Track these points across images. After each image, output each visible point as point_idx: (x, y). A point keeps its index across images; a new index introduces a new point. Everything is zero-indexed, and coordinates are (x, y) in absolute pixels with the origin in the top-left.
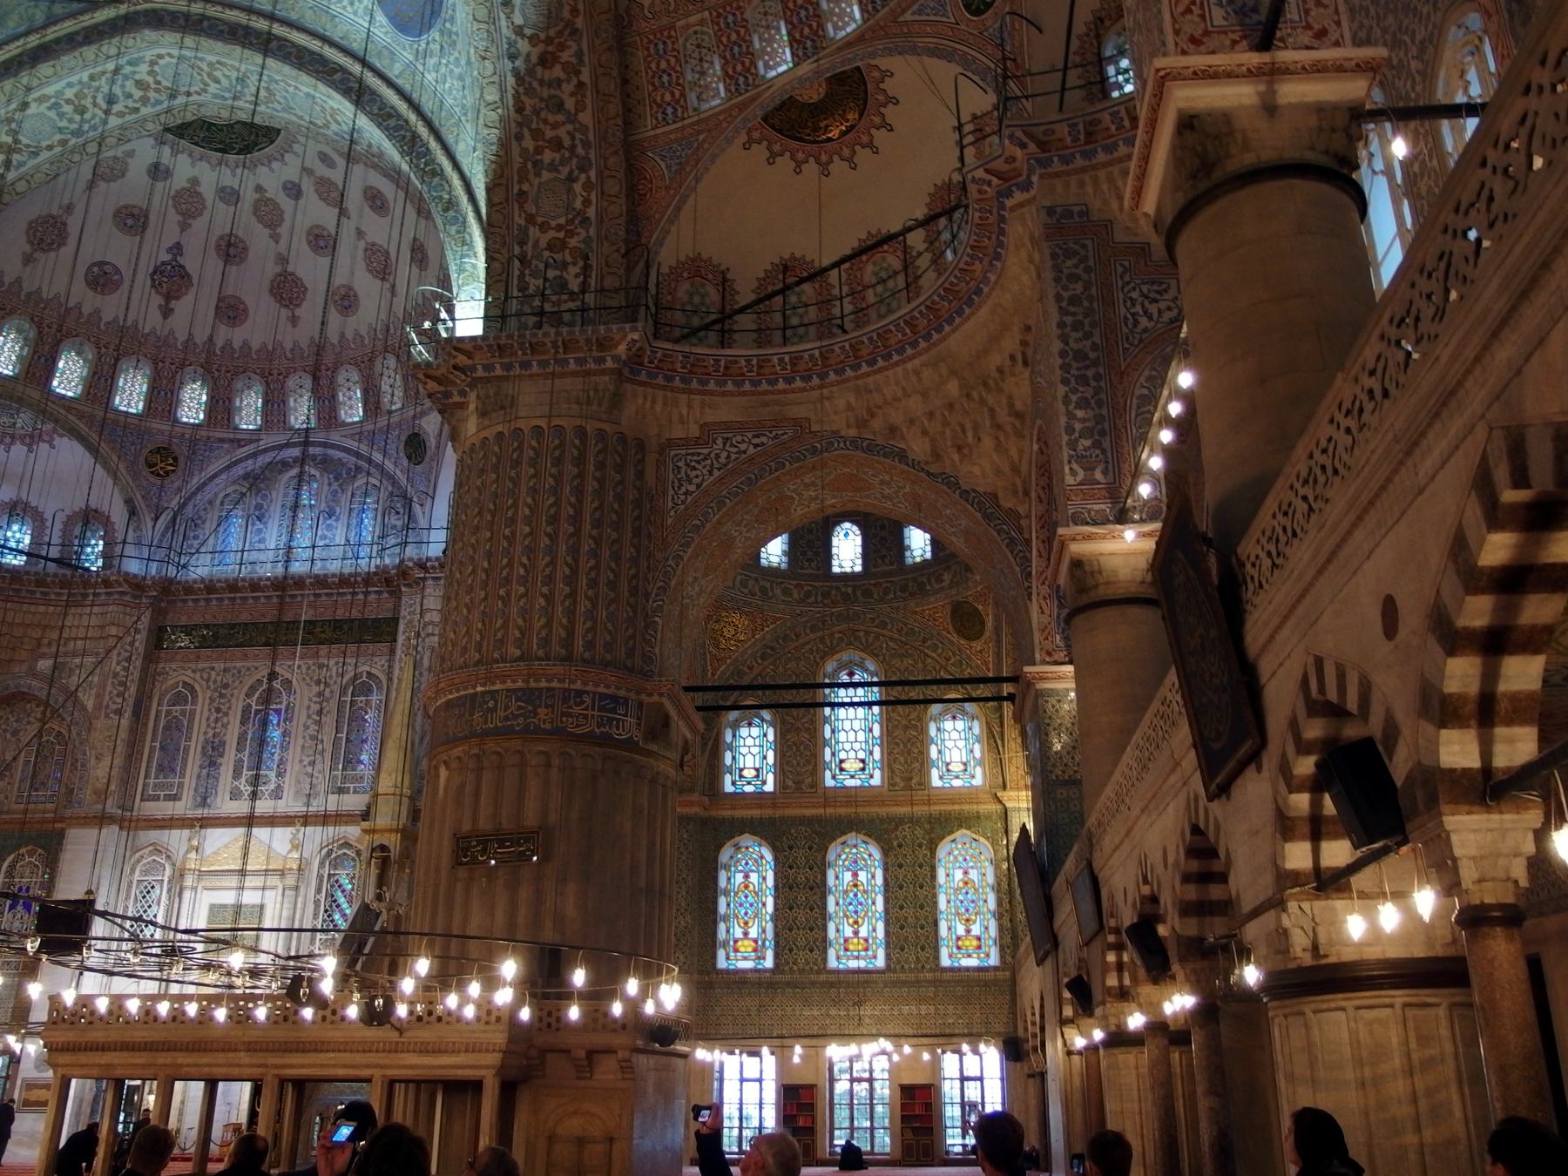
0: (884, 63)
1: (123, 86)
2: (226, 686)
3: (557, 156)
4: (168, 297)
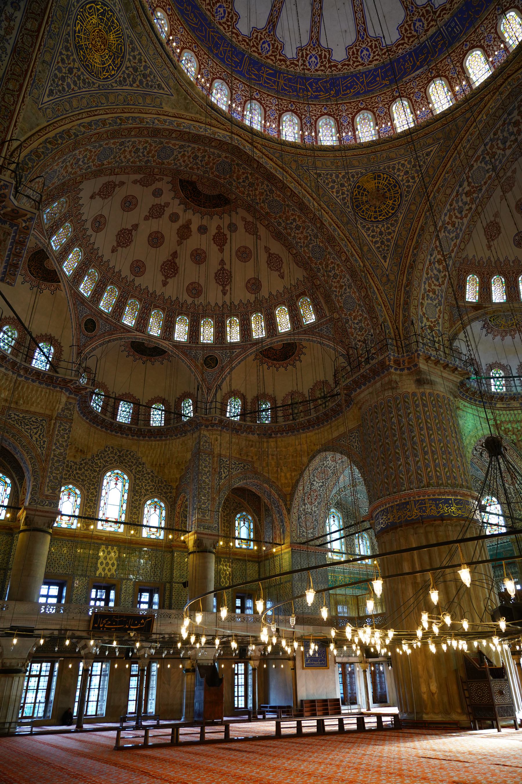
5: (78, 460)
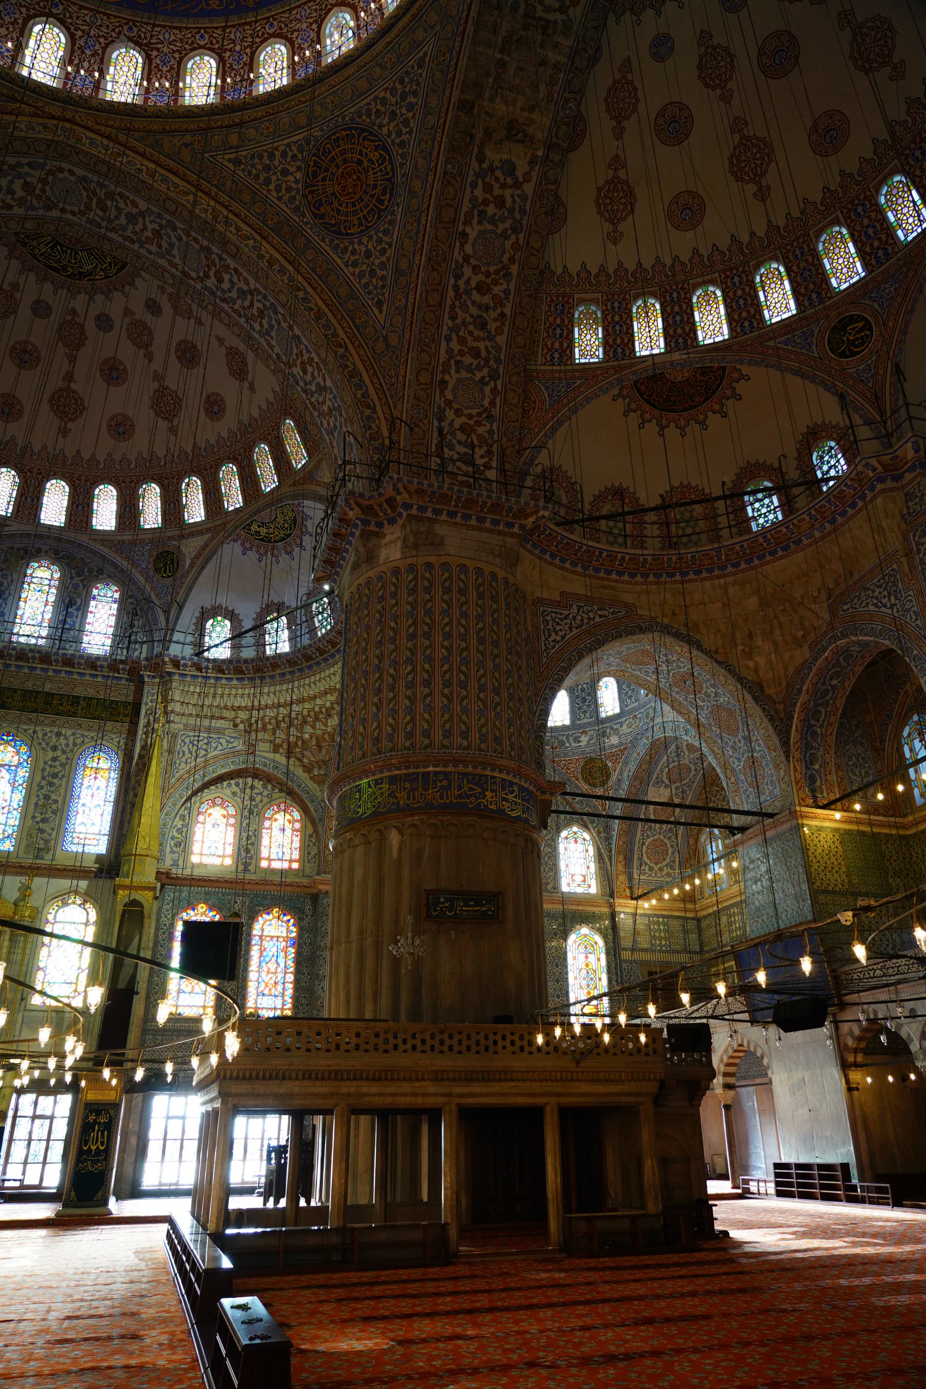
0: (745, 369)
1: (12, 182)
3: (475, 362)
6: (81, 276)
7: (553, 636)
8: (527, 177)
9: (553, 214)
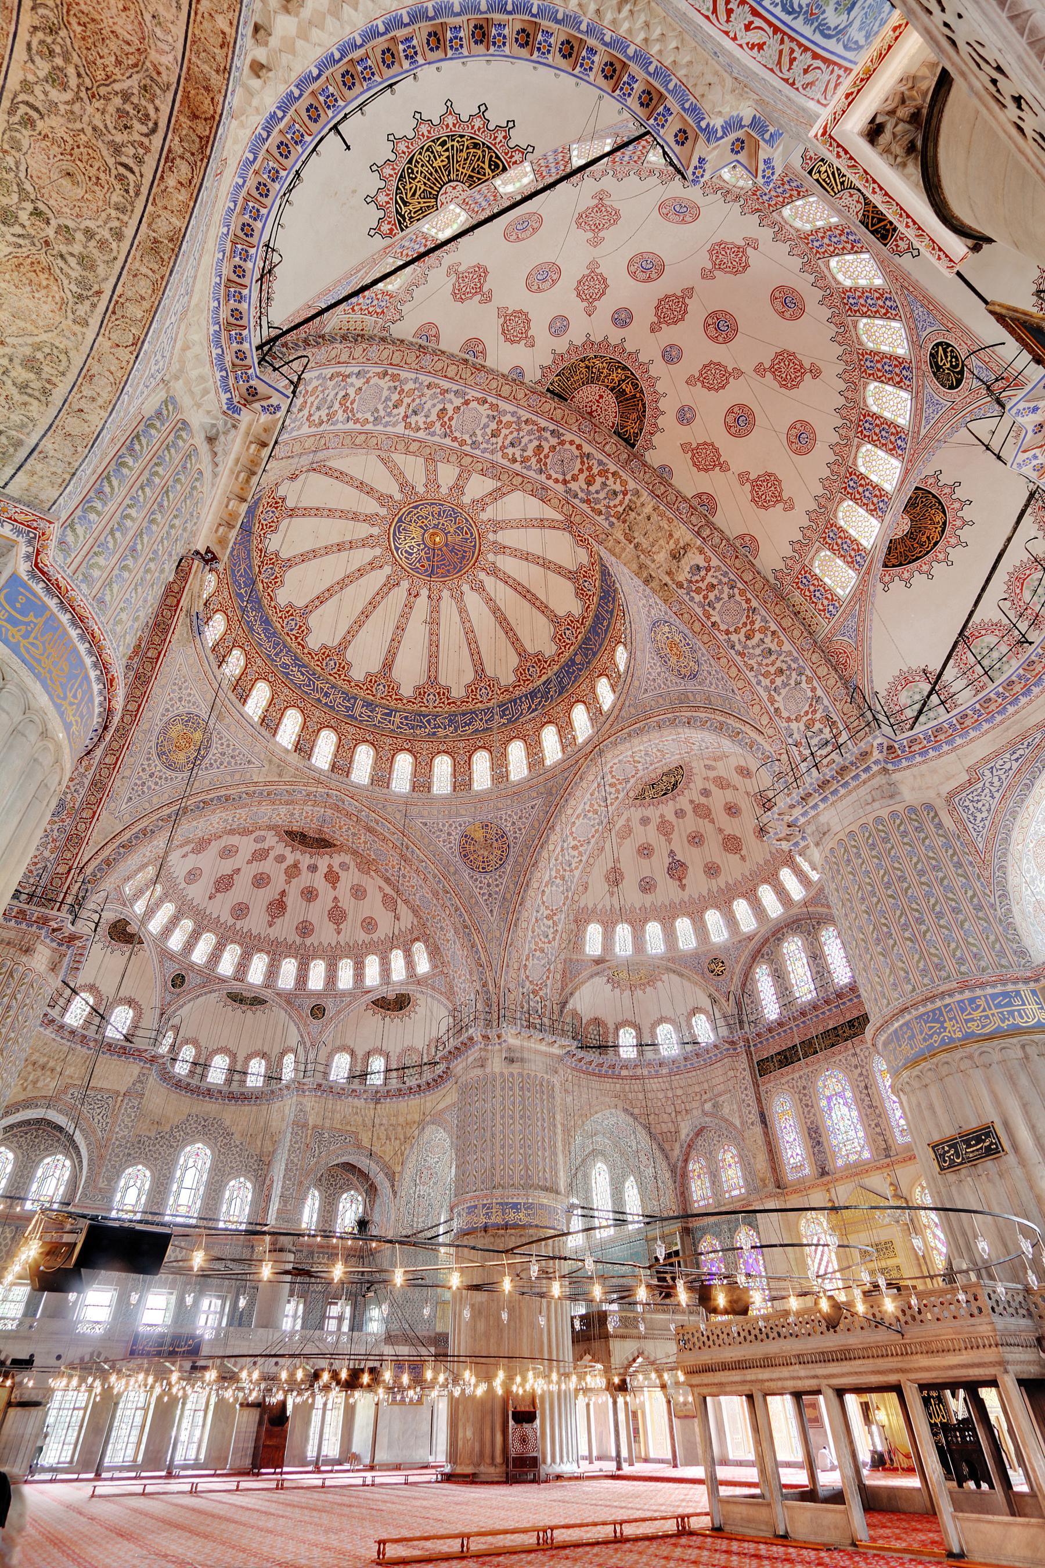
2: (804, 1088)
3: (783, 678)
4: (680, 880)
5: (153, 1135)
6: (675, 786)
7: (979, 816)
8: (708, 560)
9: (742, 550)
